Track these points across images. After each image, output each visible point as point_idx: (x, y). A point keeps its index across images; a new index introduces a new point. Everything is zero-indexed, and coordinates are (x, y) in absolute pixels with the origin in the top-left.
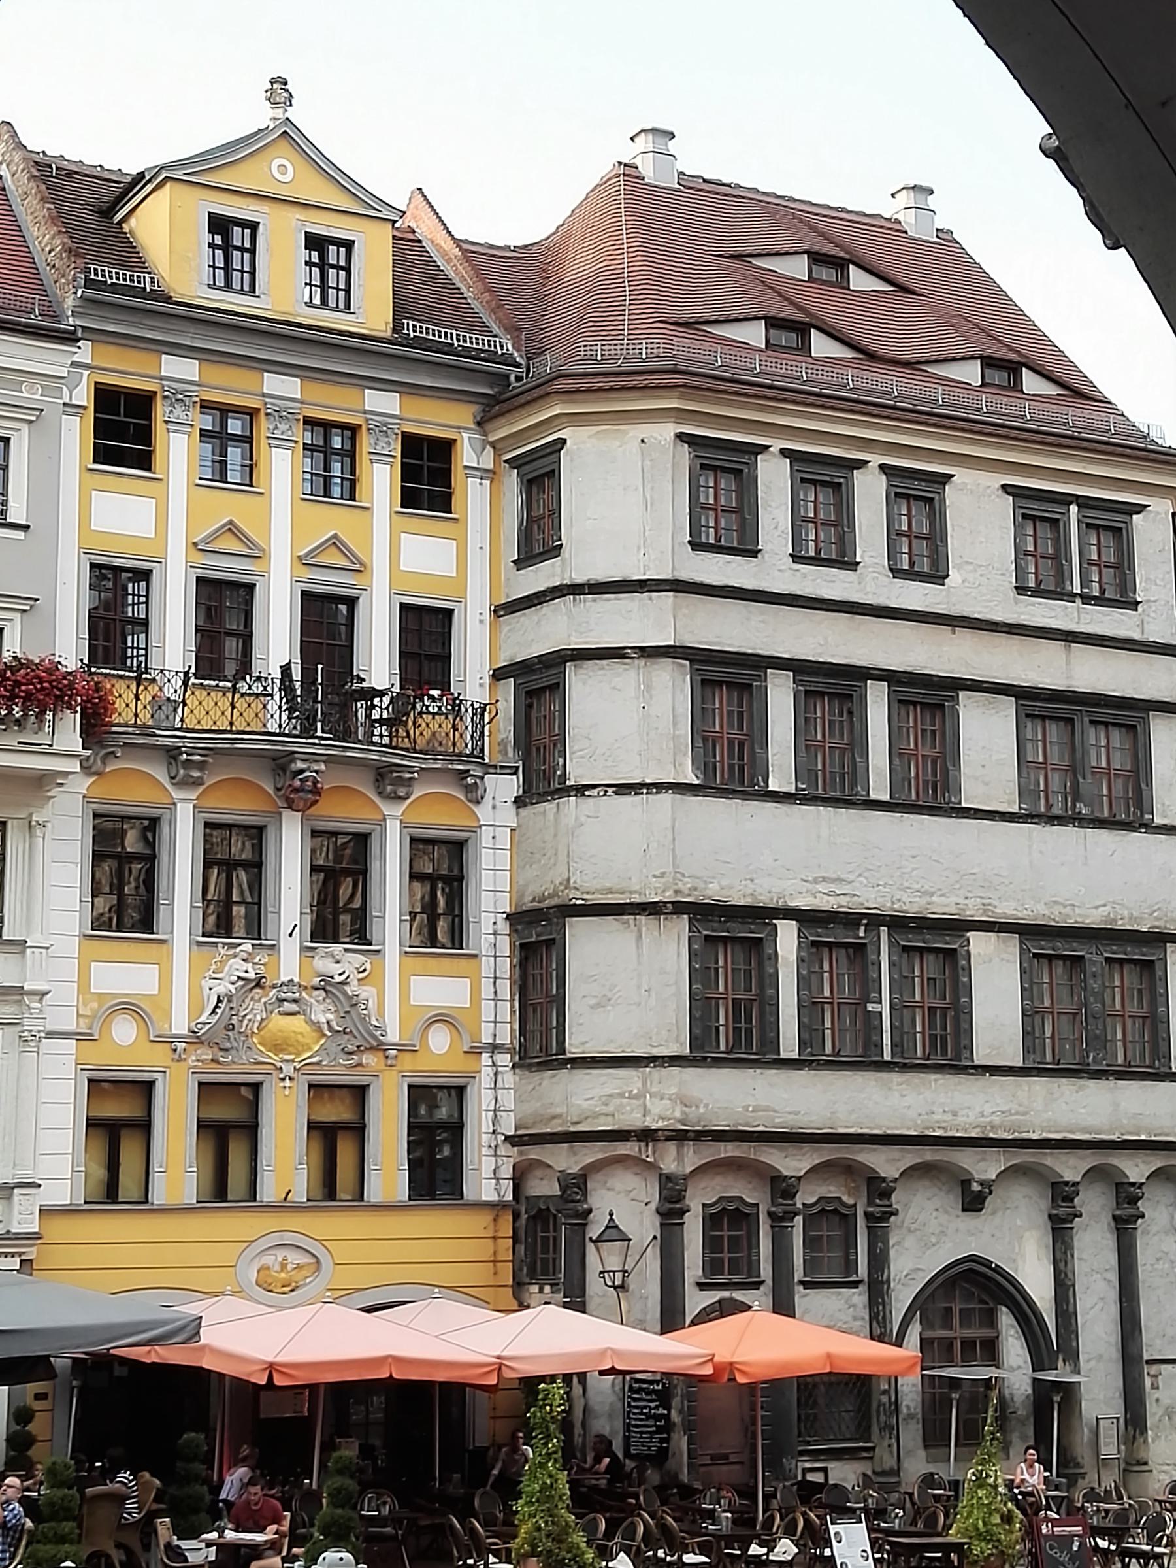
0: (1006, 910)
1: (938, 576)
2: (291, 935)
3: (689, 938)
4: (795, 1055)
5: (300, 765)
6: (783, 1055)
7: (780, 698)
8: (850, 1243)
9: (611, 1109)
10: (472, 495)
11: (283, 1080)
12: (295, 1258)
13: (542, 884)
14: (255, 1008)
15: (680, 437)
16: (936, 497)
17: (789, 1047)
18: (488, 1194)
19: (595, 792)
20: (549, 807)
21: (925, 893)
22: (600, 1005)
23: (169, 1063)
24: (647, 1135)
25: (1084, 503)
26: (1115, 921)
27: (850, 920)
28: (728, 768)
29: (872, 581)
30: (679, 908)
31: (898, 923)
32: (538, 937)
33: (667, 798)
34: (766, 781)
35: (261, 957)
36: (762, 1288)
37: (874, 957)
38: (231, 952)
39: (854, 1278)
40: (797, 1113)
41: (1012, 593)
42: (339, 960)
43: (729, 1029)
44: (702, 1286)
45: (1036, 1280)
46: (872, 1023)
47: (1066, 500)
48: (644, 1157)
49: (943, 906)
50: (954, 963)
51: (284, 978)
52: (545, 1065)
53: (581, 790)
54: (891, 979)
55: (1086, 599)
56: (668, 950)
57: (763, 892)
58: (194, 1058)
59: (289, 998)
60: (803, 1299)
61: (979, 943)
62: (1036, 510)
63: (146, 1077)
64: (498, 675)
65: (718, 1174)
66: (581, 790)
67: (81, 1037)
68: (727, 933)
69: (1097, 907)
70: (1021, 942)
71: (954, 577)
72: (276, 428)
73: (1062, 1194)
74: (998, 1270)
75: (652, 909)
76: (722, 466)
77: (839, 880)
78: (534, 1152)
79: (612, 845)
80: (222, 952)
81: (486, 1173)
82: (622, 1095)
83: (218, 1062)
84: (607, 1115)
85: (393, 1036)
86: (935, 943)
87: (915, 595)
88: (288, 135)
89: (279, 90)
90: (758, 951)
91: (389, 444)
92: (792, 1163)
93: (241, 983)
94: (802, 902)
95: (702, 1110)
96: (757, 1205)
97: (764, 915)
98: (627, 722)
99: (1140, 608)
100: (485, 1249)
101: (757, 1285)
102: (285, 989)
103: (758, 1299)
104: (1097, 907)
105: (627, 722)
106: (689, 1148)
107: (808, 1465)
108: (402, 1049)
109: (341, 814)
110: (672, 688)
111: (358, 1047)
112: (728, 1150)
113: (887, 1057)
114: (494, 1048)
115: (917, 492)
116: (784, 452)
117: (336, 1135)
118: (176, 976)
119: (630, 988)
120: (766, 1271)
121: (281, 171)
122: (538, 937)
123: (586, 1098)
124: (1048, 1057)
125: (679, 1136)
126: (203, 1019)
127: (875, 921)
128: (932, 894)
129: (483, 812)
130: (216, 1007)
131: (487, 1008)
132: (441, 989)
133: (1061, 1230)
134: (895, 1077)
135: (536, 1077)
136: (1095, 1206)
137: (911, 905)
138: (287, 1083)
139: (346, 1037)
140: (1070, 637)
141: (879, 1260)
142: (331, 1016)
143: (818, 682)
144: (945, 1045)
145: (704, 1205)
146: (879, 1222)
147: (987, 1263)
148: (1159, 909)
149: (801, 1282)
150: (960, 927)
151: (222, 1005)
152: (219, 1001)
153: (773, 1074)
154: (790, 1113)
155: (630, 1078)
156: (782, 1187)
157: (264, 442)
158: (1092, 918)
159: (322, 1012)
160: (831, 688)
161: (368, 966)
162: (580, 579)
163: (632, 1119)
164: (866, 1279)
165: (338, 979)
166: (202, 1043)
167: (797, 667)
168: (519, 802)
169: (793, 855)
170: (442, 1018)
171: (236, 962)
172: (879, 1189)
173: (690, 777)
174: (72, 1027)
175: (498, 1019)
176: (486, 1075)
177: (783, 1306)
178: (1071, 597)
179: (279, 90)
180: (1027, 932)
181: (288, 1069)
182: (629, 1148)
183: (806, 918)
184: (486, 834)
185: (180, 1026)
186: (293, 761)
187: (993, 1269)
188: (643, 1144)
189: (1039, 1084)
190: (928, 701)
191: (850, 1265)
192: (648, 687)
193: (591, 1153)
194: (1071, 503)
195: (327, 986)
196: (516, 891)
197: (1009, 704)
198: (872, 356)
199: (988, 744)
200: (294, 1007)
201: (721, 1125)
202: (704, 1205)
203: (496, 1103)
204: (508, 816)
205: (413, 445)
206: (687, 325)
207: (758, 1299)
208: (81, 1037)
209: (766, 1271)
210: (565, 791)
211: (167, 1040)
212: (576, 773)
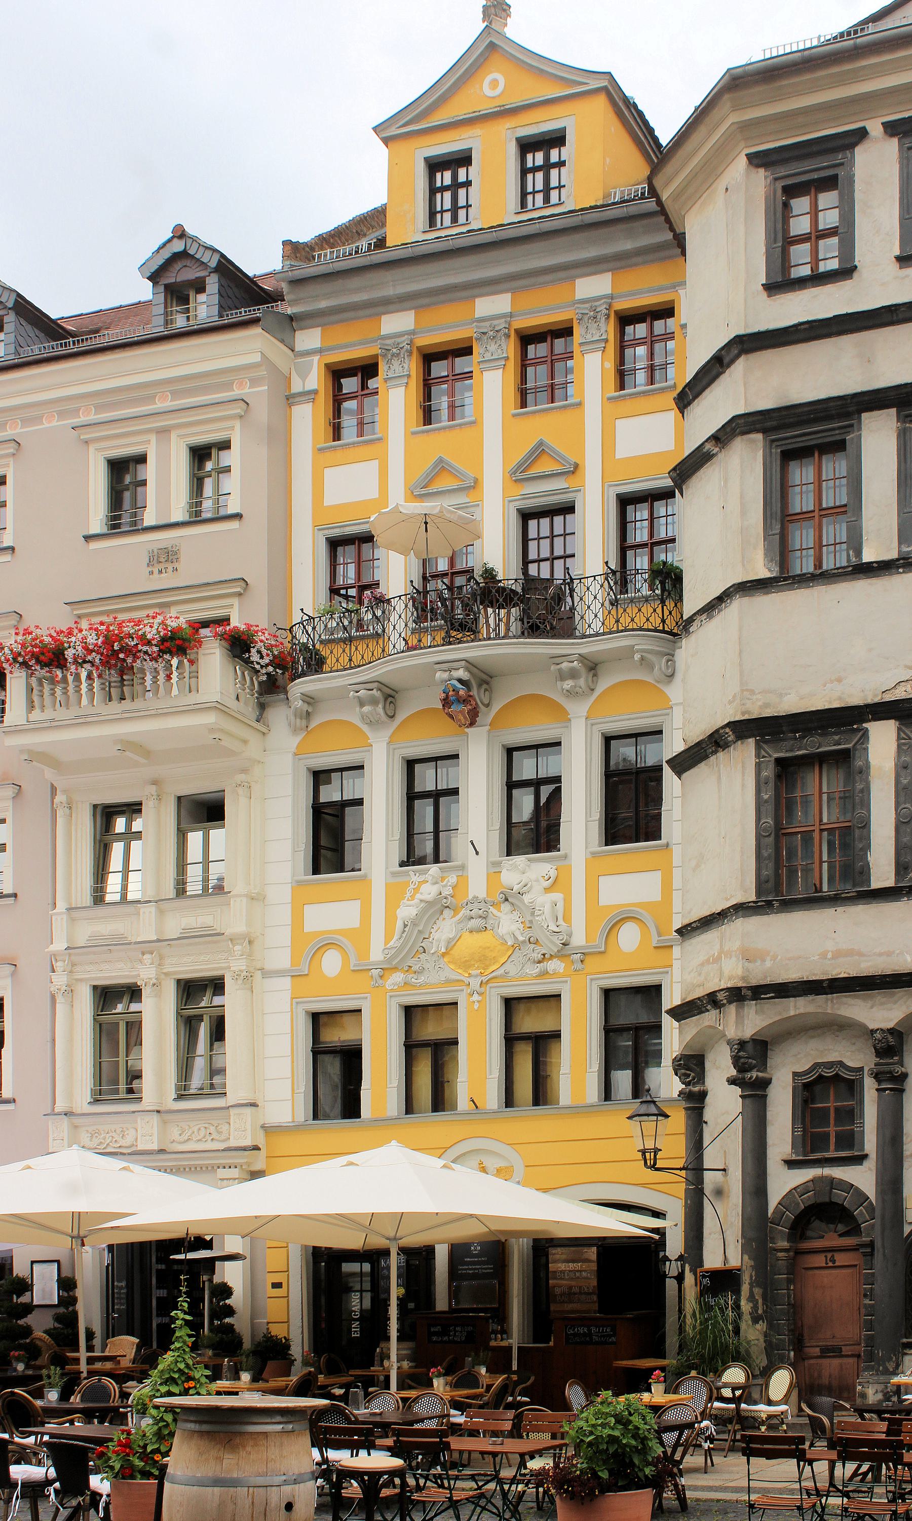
4: (890, 882)
6: (875, 884)
14: (445, 929)
33: (737, 605)
36: (866, 1163)
40: (889, 954)
44: (791, 1164)
65: (813, 1037)
82: (708, 961)
84: (699, 986)
95: (768, 964)
96: (861, 1069)
101: (860, 1159)
111: (544, 955)
120: (870, 1143)
139: (532, 946)
145: (795, 1074)
154: (880, 954)
171: (428, 882)
173: (762, 572)
188: (718, 1011)
202: (795, 1074)
209: (870, 1143)
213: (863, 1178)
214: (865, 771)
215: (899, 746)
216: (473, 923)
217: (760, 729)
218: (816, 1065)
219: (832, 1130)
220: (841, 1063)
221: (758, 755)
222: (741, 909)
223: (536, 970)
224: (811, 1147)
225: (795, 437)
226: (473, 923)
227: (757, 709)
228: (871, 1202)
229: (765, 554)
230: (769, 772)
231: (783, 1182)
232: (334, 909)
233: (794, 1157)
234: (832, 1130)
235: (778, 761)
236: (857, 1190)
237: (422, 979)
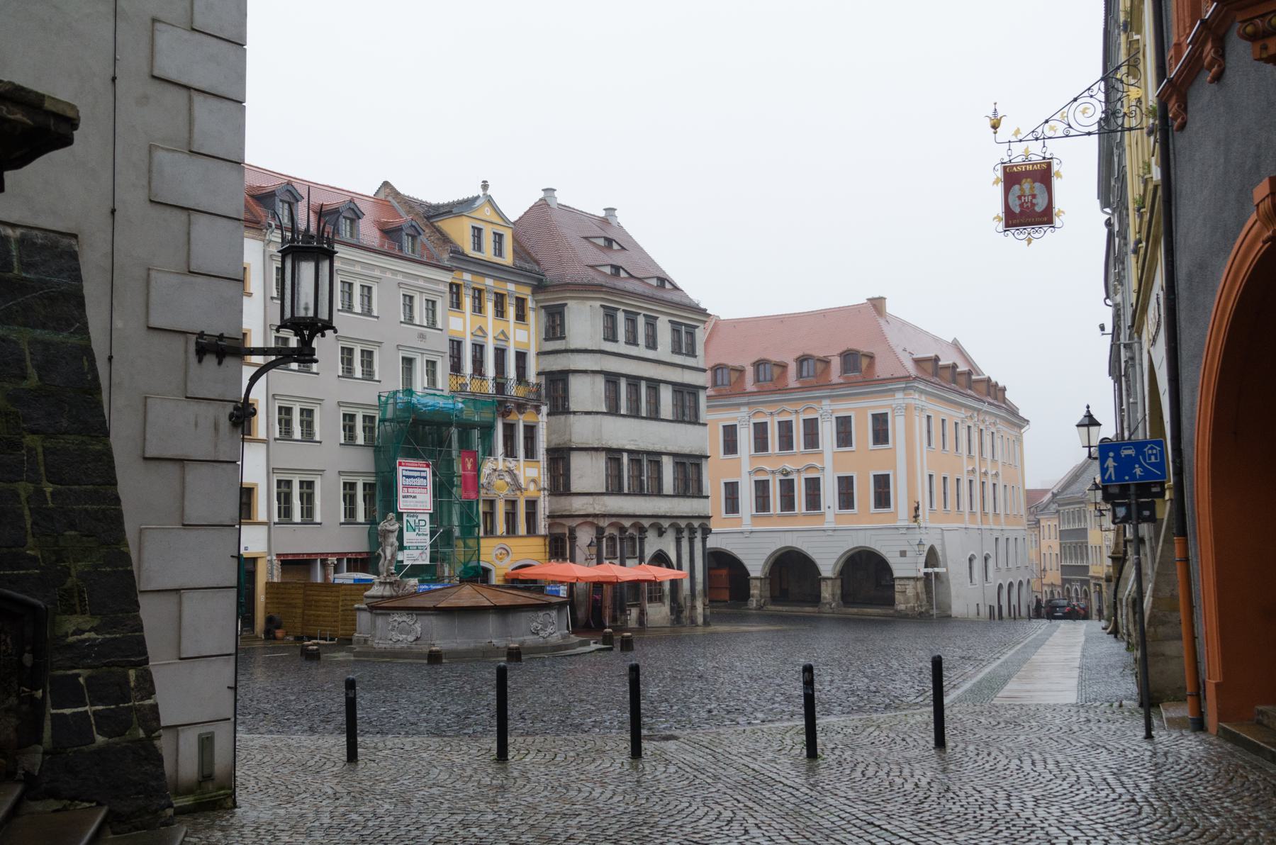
8: (634, 547)
10: (531, 316)
13: (557, 441)
17: (626, 491)
20: (562, 418)
24: (596, 516)
25: (686, 325)
29: (641, 351)
32: (559, 458)
33: (599, 417)
42: (511, 463)
43: (615, 488)
46: (641, 482)
47: (681, 324)
49: (657, 448)
50: (658, 464)
52: (562, 495)
53: (574, 413)
56: (600, 462)
57: (658, 447)
60: (628, 562)
64: (539, 374)
66: (574, 413)
68: (613, 455)
73: (679, 531)
75: (596, 449)
76: (610, 314)
78: (558, 520)
79: (582, 430)
81: (542, 528)
86: (655, 457)
87: (650, 354)
88: (490, 201)
89: (485, 186)
90: (618, 461)
92: (627, 523)
94: (628, 447)
97: (620, 451)
100: (542, 549)
103: (617, 561)
105: (585, 393)
109: (511, 418)
110: (600, 382)
112: (614, 520)
115: (651, 323)
117: (511, 517)
121: (487, 213)
122: (559, 458)
123: (578, 505)
125: (604, 516)
133: (678, 541)
135: (558, 499)
136: (686, 534)
137: (651, 448)
140: (683, 367)
141: (642, 551)
143: (631, 381)
146: (642, 540)
150: (660, 454)
153: (623, 498)
156: (622, 529)
158: (687, 451)
162: (572, 347)
163: (590, 511)
168: (549, 414)
169: (627, 433)
170: (534, 481)
172: (642, 530)
173: (605, 410)
175: (544, 482)
177: (623, 564)
179: (485, 186)
180: (674, 455)
182: (590, 519)
183: (630, 452)
189: (676, 500)
191: (634, 552)
193: (579, 521)
196: (549, 442)
197: (670, 387)
198: (631, 276)
201: (612, 512)
203: (544, 506)
205: (517, 298)
206: (592, 267)
207: (617, 561)
210: (570, 413)
212: (573, 407)
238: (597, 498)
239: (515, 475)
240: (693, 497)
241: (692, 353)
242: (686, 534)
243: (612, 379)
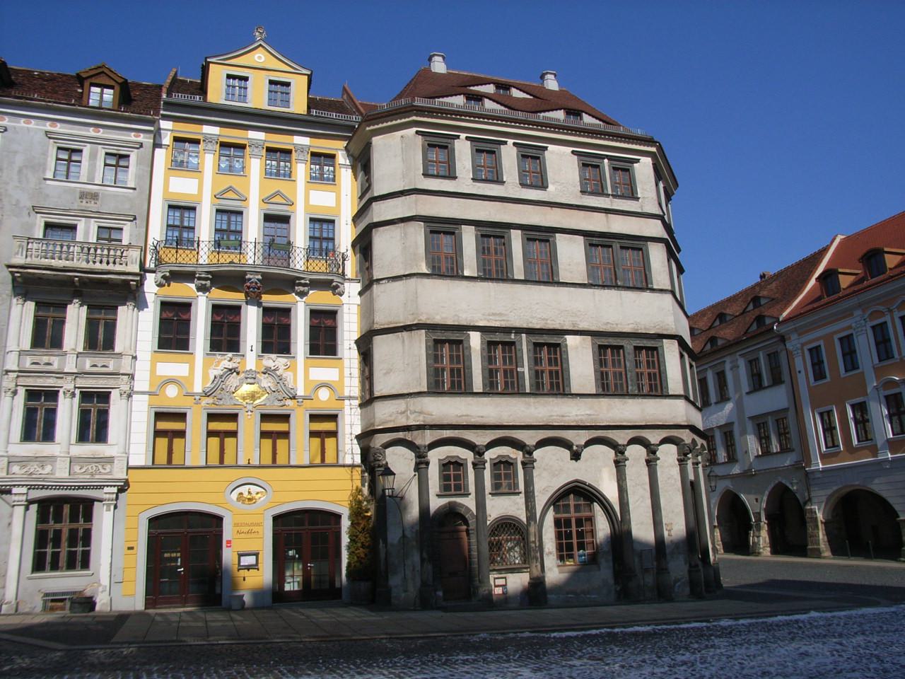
0: (583, 326)
1: (543, 186)
2: (252, 350)
3: (426, 340)
5: (248, 276)
7: (469, 237)
9: (392, 418)
11: (247, 412)
12: (254, 489)
14: (233, 380)
15: (417, 132)
16: (541, 156)
18: (348, 461)
19: (384, 281)
21: (543, 319)
22: (387, 373)
23: (193, 405)
24: (407, 428)
26: (637, 330)
27: (507, 330)
28: (445, 267)
30: (419, 326)
31: (530, 331)
33: (413, 280)
34: (463, 272)
35: (238, 359)
36: (470, 496)
37: (520, 347)
38: (223, 358)
39: (517, 491)
40: (482, 417)
41: (579, 194)
45: (609, 490)
47: (602, 157)
48: (407, 438)
51: (248, 369)
54: (529, 358)
55: (614, 196)
56: (418, 344)
58: (204, 402)
59: (251, 377)
61: (571, 340)
62: (589, 163)
63: (182, 411)
66: (378, 281)
67: (150, 394)
68: (446, 340)
69: (628, 324)
70: (592, 340)
71: (551, 188)
72: (253, 151)
74: (590, 486)
76: (438, 145)
77: (500, 314)
79: (393, 303)
80: (219, 357)
83: (216, 405)
85: (300, 392)
86: (549, 343)
91: (304, 156)
93: (226, 370)
98: (399, 249)
99: (640, 200)
101: (467, 495)
102: (248, 373)
104: (628, 324)
106: (428, 432)
107: (496, 576)
108: (305, 398)
110: (418, 233)
113: (528, 391)
114: (350, 398)
116: (467, 138)
118: (197, 367)
119: (403, 363)
120: (472, 488)
124: (607, 387)
126: (207, 386)
127: (519, 331)
128: (547, 320)
129: (344, 299)
130: (214, 381)
131: (347, 381)
132: (324, 371)
133: (619, 464)
134: (531, 400)
136: (636, 454)
138: (249, 413)
140: (607, 211)
142: (269, 384)
143: (489, 230)
144: (554, 383)
145: (439, 460)
146: (528, 465)
147: (584, 483)
148: (658, 325)
149: (490, 494)
151: (217, 380)
152: (215, 377)
153: (469, 399)
154: (479, 417)
155: (400, 404)
157: (248, 156)
159: (266, 382)
160: (493, 233)
161: (288, 363)
163: (402, 422)
164: (523, 491)
165: (273, 368)
166: (208, 396)
167: (476, 223)
168: (360, 294)
171: (225, 361)
174: (147, 389)
175: (353, 386)
176: (347, 410)
178: (608, 195)
181: (250, 407)
183: (483, 330)
184: (345, 308)
185: (198, 389)
186: (247, 275)
187: (588, 486)
190: (540, 236)
192: (405, 234)
194: (604, 158)
195: (267, 371)
197: (580, 239)
199: (571, 255)
200: (252, 381)
201: (445, 422)
202: (439, 460)
204: (358, 300)
208: (150, 394)
209: (472, 488)
211: (192, 395)
213: (469, 503)
214: (469, 347)
215: (482, 341)
216: (249, 381)
217: (430, 327)
218: (448, 457)
219: (452, 483)
220: (458, 457)
221: (426, 336)
222: (420, 394)
223: (277, 403)
224: (445, 489)
225: (436, 226)
226: (249, 381)
227: (424, 319)
228: (473, 513)
229: (426, 265)
230: (431, 344)
231: (436, 503)
232: (173, 366)
233: (439, 493)
234: (452, 483)
235: (434, 340)
236: (467, 507)
237: (221, 402)
238: (410, 400)
239: (280, 378)
240: (634, 396)
241: (633, 196)
242: (636, 454)
243: (441, 228)
